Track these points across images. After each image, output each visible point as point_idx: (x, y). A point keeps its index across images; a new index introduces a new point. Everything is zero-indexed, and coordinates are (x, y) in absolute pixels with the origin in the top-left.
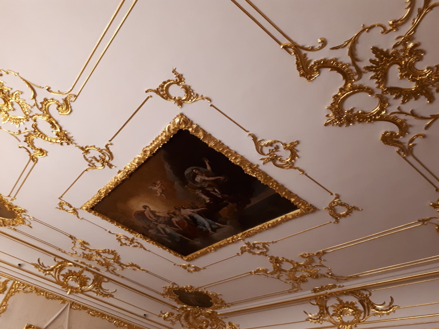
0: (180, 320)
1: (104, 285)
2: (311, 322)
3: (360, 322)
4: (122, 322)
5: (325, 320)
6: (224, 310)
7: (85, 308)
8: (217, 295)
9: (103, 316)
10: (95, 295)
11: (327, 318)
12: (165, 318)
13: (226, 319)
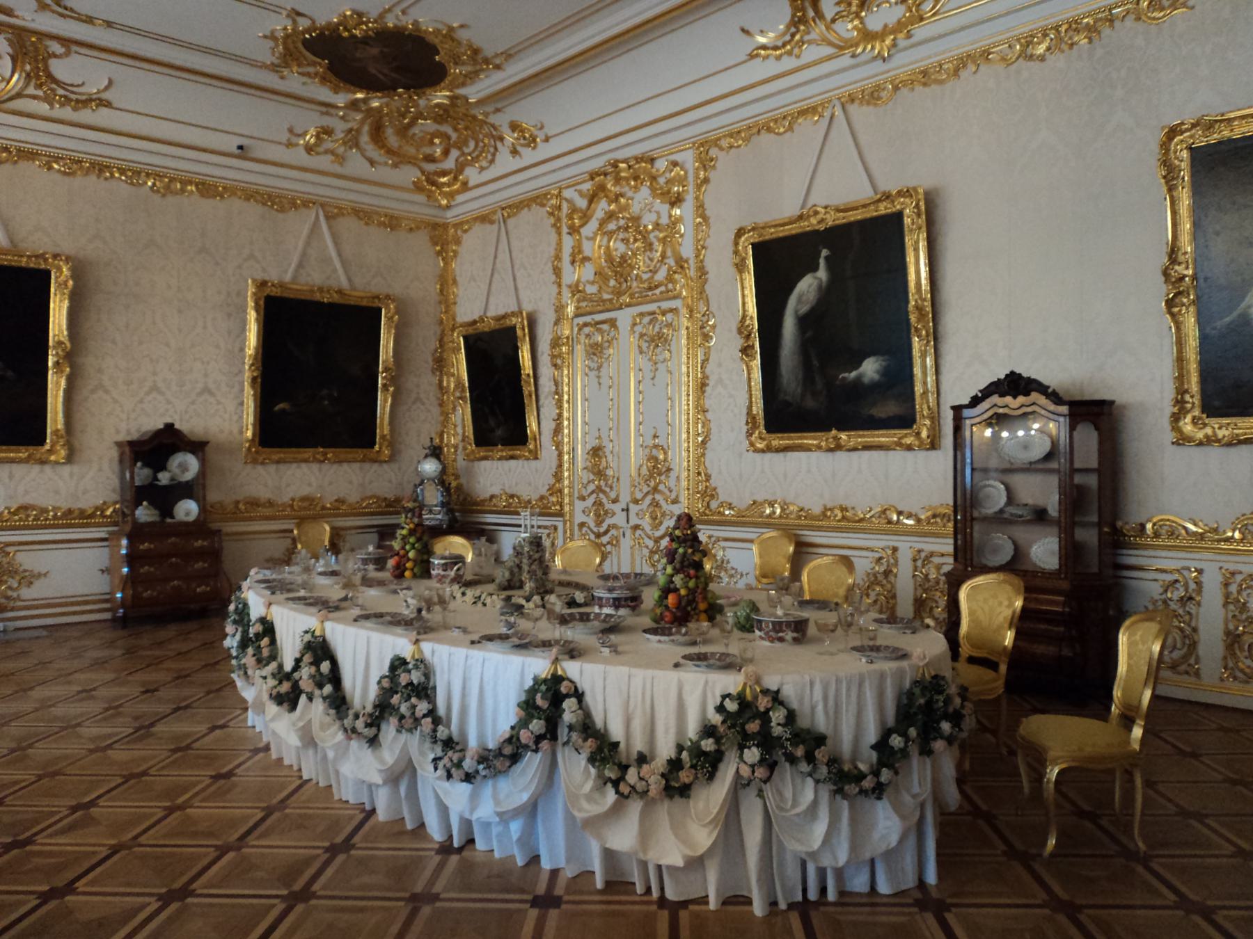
0: (357, 145)
1: (59, 69)
2: (767, 57)
3: (922, 19)
4: (172, 180)
5: (810, 42)
6: (487, 82)
7: (31, 155)
8: (451, 29)
9: (101, 171)
10: (43, 108)
11: (819, 30)
12: (309, 149)
13: (499, 114)
